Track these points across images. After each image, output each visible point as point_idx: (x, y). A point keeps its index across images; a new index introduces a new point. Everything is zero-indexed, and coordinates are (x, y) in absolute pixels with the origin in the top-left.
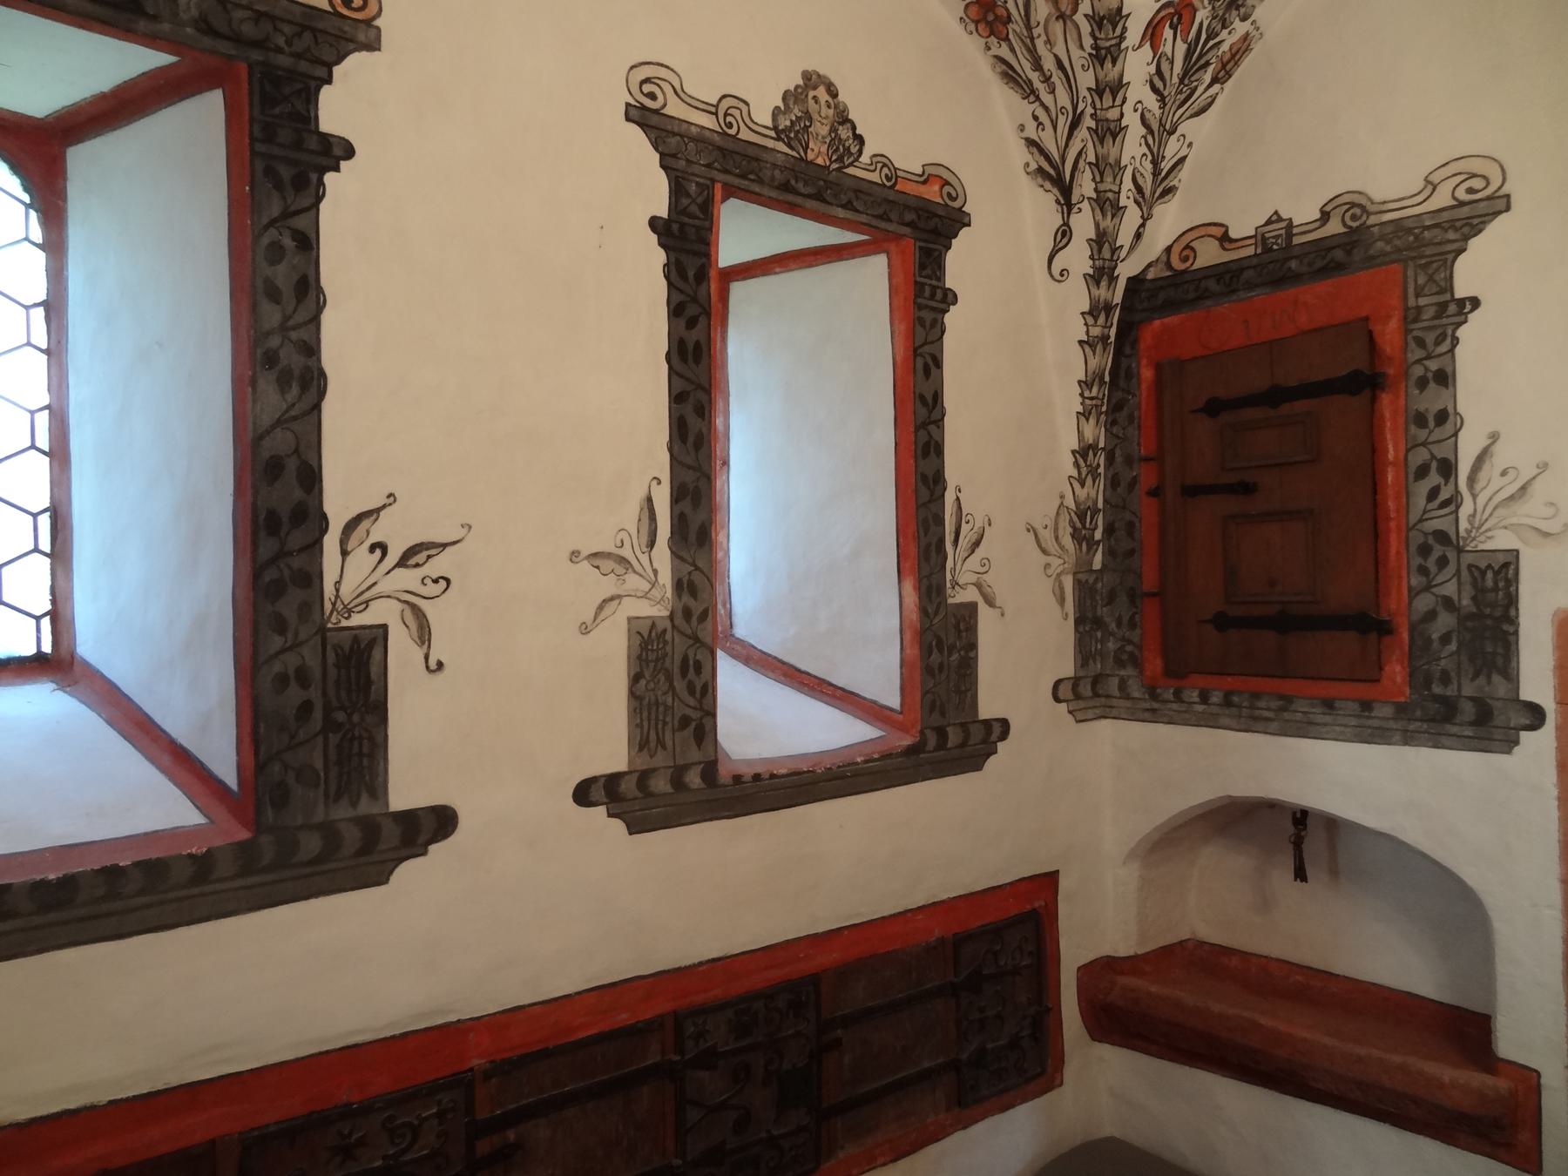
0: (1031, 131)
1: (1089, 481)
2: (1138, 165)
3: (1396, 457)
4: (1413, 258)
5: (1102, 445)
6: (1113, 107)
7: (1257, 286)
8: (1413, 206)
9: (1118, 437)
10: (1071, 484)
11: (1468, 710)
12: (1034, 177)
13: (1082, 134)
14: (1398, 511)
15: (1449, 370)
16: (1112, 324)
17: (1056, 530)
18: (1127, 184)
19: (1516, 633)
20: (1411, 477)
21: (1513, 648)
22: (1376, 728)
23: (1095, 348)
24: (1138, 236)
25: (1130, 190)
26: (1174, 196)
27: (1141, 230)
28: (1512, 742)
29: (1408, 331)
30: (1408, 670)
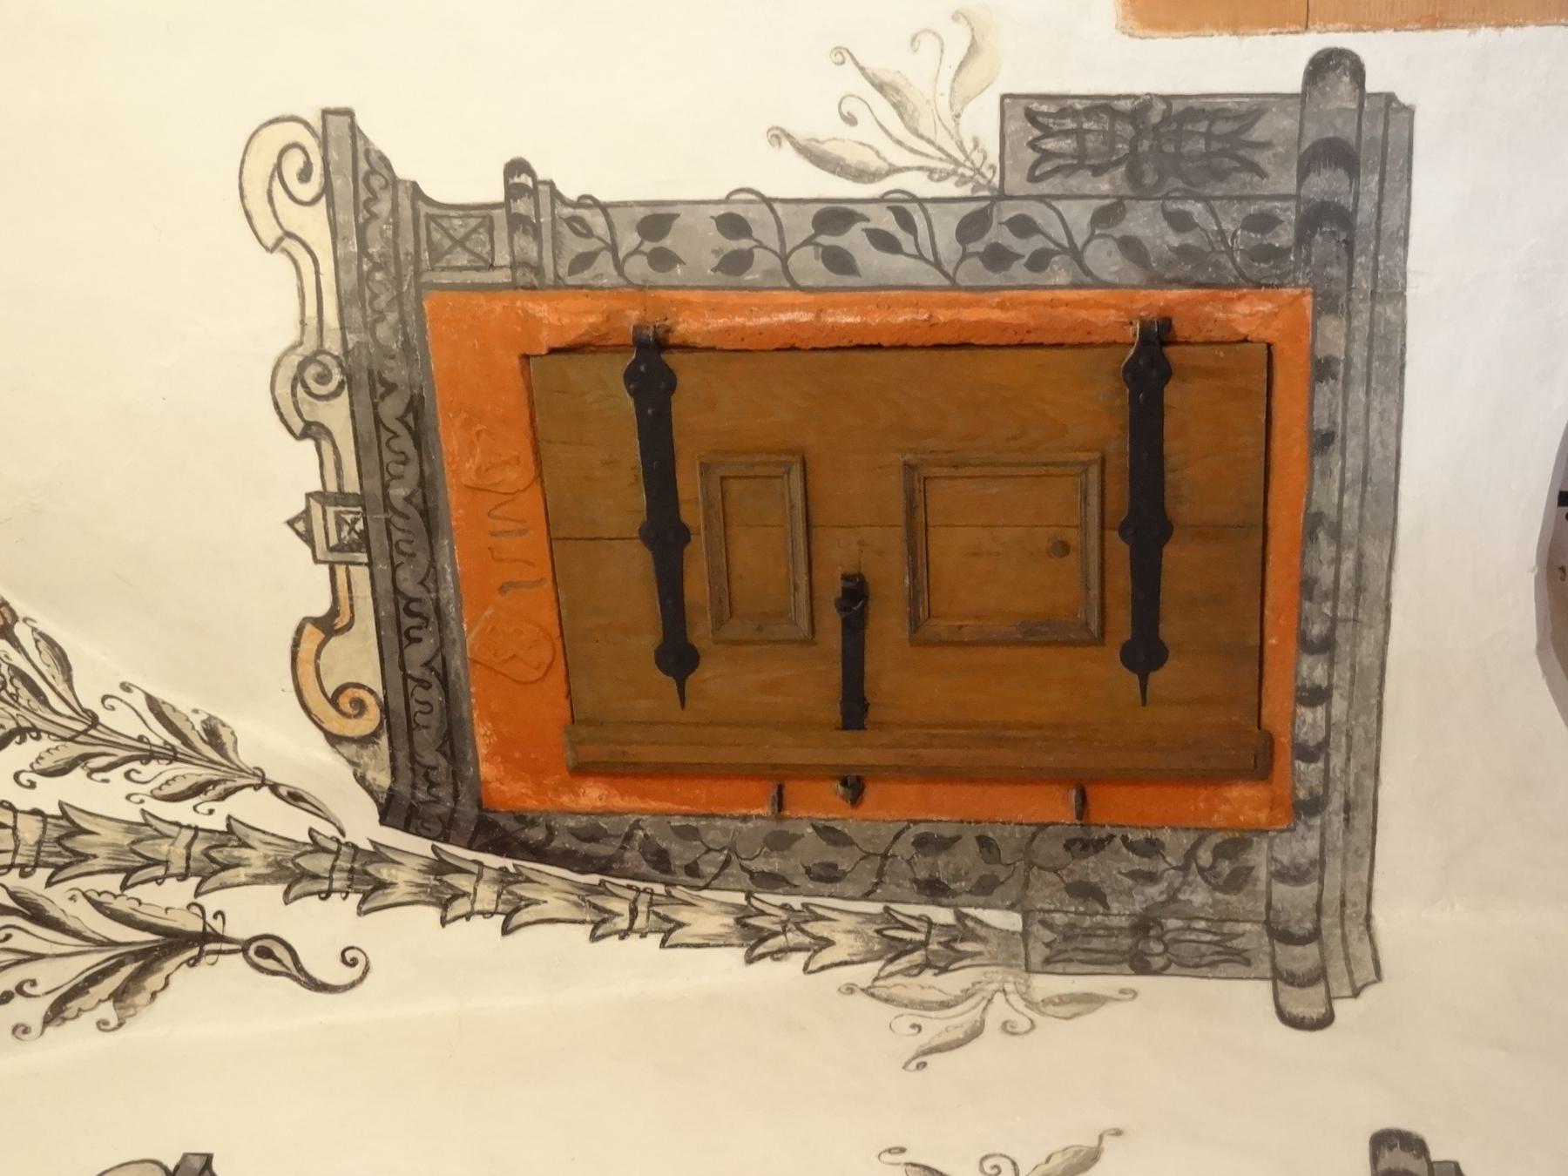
0: (31, 1010)
1: (817, 928)
2: (146, 789)
3: (804, 307)
4: (418, 273)
5: (740, 898)
6: (14, 828)
7: (433, 563)
8: (317, 273)
9: (727, 863)
10: (823, 968)
11: (1325, 183)
12: (131, 1012)
13: (58, 900)
14: (917, 306)
15: (642, 213)
16: (475, 862)
17: (925, 1006)
18: (182, 812)
19: (1167, 99)
20: (849, 281)
21: (1195, 103)
22: (1370, 349)
23: (521, 898)
24: (295, 798)
25: (195, 808)
26: (224, 725)
27: (283, 791)
28: (1388, 105)
29: (559, 285)
30: (1245, 290)
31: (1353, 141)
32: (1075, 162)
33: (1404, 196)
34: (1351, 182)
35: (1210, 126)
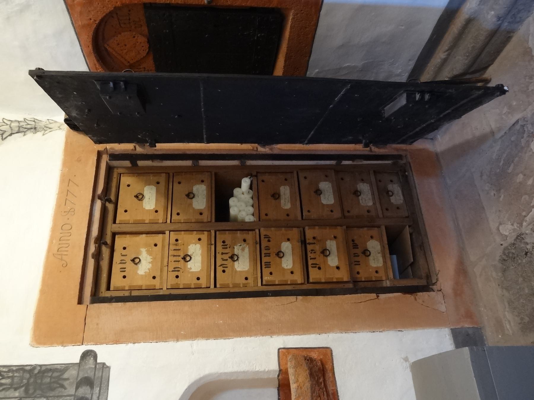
19: (41, 366)
21: (49, 367)
28: (103, 367)
31: (93, 377)
32: (10, 386)
33: (106, 394)
34: (91, 390)
35: (52, 375)
